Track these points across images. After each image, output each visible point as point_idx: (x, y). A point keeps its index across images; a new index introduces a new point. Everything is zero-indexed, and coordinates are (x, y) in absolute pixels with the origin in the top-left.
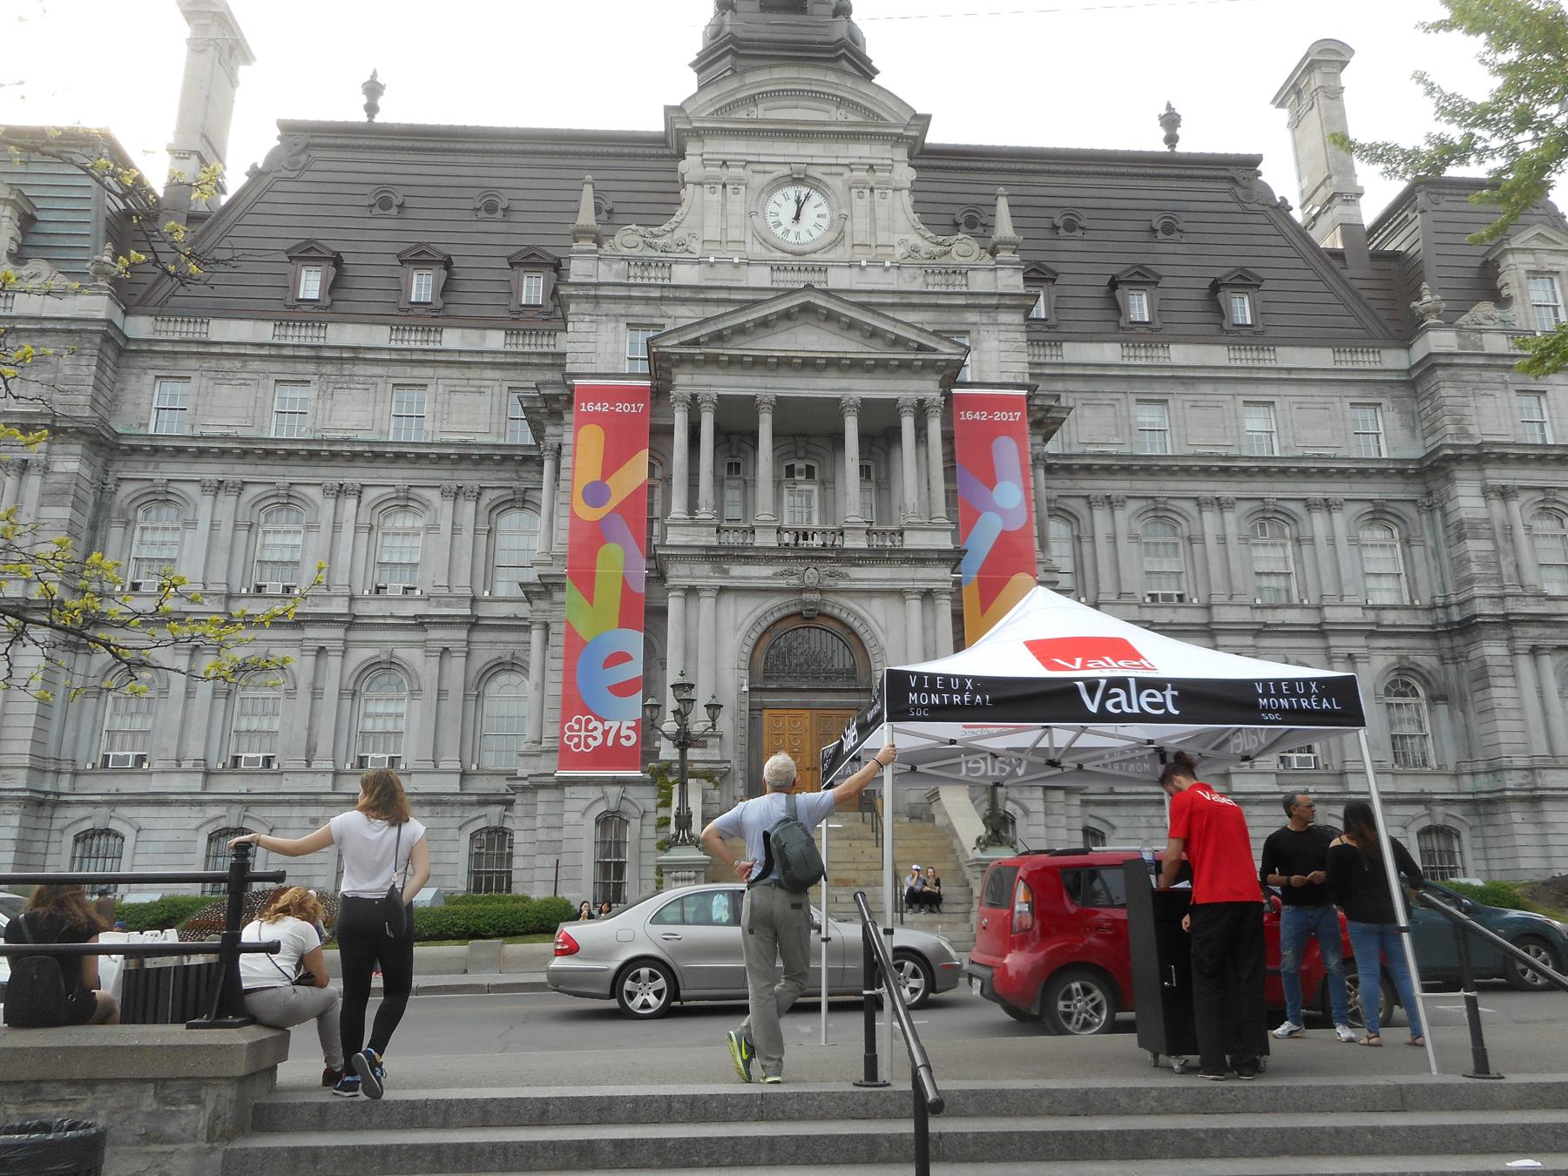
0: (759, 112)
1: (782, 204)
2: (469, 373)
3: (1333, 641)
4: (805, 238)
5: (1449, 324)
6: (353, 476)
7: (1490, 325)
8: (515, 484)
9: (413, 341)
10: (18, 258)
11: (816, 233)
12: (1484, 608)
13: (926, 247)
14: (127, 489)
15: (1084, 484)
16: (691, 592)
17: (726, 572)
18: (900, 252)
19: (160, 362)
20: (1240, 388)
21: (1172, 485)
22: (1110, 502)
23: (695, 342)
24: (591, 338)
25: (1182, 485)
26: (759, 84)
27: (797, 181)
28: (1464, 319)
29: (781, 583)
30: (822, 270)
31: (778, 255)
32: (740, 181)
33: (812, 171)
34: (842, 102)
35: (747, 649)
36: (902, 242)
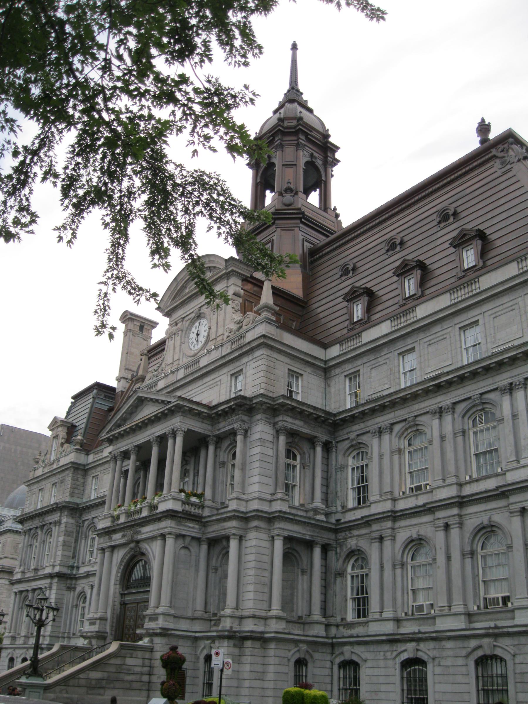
0: (187, 290)
3: (513, 499)
10: (62, 445)
14: (86, 523)
15: (370, 423)
16: (103, 550)
17: (111, 538)
19: (93, 471)
20: (457, 320)
21: (416, 407)
22: (380, 432)
23: (111, 430)
25: (423, 405)
26: (182, 279)
27: (199, 317)
29: (123, 541)
35: (119, 575)
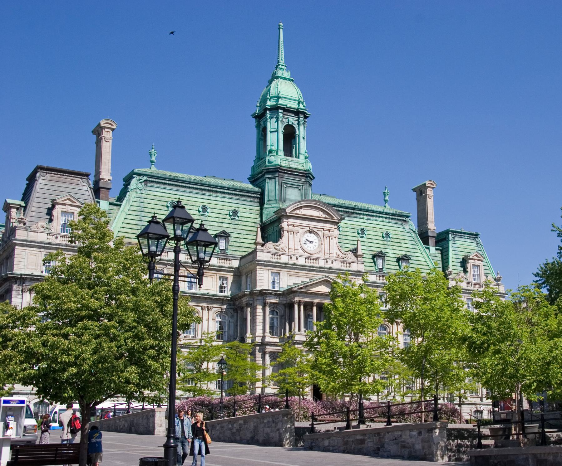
4: (312, 249)
11: (315, 248)
13: (341, 255)
18: (335, 255)
23: (301, 288)
24: (263, 275)
27: (310, 232)
31: (306, 254)
33: (315, 230)
36: (336, 253)
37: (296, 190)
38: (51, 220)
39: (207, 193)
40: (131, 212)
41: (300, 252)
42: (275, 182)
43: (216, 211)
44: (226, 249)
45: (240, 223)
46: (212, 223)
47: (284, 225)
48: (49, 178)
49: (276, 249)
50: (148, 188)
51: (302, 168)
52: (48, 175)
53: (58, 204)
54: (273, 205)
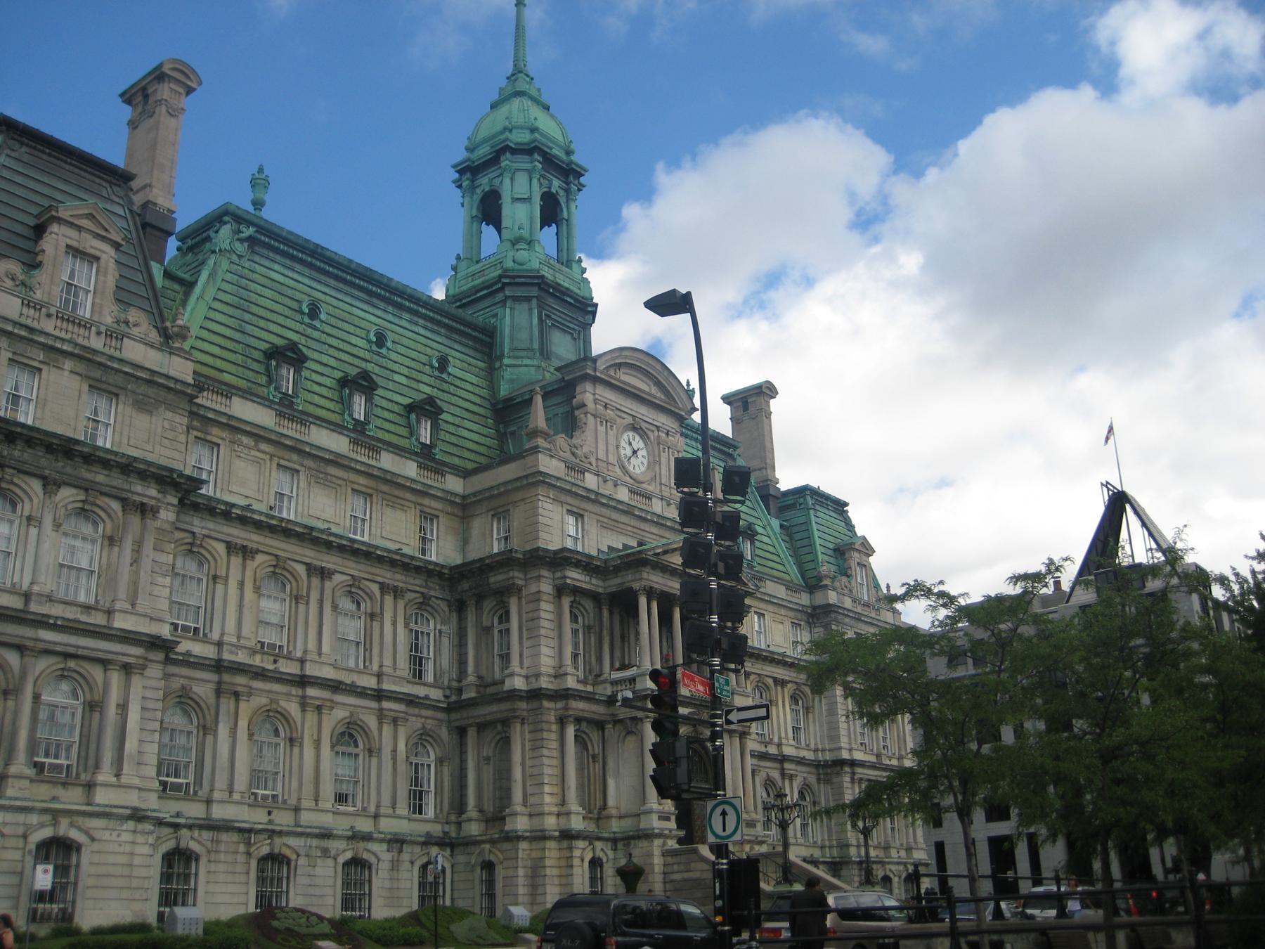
1: (630, 442)
2: (397, 493)
4: (637, 471)
5: (834, 590)
6: (329, 561)
7: (846, 591)
8: (425, 591)
9: (362, 457)
11: (643, 469)
12: (845, 755)
26: (626, 357)
27: (634, 428)
28: (837, 584)
30: (650, 499)
31: (628, 479)
32: (613, 422)
34: (658, 384)
37: (568, 338)
38: (33, 265)
39: (382, 305)
40: (217, 305)
41: (618, 470)
42: (530, 309)
43: (403, 350)
44: (432, 446)
45: (452, 389)
46: (397, 378)
47: (588, 398)
48: (26, 158)
49: (573, 454)
50: (257, 258)
51: (577, 291)
52: (24, 149)
53: (59, 220)
54: (526, 362)
